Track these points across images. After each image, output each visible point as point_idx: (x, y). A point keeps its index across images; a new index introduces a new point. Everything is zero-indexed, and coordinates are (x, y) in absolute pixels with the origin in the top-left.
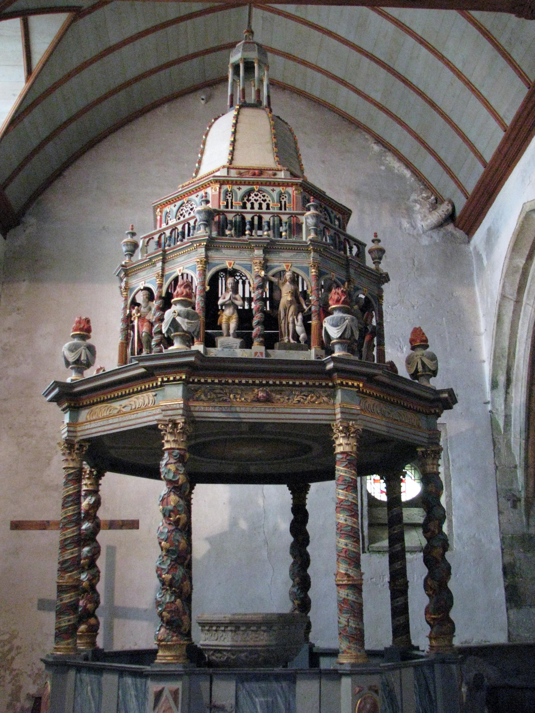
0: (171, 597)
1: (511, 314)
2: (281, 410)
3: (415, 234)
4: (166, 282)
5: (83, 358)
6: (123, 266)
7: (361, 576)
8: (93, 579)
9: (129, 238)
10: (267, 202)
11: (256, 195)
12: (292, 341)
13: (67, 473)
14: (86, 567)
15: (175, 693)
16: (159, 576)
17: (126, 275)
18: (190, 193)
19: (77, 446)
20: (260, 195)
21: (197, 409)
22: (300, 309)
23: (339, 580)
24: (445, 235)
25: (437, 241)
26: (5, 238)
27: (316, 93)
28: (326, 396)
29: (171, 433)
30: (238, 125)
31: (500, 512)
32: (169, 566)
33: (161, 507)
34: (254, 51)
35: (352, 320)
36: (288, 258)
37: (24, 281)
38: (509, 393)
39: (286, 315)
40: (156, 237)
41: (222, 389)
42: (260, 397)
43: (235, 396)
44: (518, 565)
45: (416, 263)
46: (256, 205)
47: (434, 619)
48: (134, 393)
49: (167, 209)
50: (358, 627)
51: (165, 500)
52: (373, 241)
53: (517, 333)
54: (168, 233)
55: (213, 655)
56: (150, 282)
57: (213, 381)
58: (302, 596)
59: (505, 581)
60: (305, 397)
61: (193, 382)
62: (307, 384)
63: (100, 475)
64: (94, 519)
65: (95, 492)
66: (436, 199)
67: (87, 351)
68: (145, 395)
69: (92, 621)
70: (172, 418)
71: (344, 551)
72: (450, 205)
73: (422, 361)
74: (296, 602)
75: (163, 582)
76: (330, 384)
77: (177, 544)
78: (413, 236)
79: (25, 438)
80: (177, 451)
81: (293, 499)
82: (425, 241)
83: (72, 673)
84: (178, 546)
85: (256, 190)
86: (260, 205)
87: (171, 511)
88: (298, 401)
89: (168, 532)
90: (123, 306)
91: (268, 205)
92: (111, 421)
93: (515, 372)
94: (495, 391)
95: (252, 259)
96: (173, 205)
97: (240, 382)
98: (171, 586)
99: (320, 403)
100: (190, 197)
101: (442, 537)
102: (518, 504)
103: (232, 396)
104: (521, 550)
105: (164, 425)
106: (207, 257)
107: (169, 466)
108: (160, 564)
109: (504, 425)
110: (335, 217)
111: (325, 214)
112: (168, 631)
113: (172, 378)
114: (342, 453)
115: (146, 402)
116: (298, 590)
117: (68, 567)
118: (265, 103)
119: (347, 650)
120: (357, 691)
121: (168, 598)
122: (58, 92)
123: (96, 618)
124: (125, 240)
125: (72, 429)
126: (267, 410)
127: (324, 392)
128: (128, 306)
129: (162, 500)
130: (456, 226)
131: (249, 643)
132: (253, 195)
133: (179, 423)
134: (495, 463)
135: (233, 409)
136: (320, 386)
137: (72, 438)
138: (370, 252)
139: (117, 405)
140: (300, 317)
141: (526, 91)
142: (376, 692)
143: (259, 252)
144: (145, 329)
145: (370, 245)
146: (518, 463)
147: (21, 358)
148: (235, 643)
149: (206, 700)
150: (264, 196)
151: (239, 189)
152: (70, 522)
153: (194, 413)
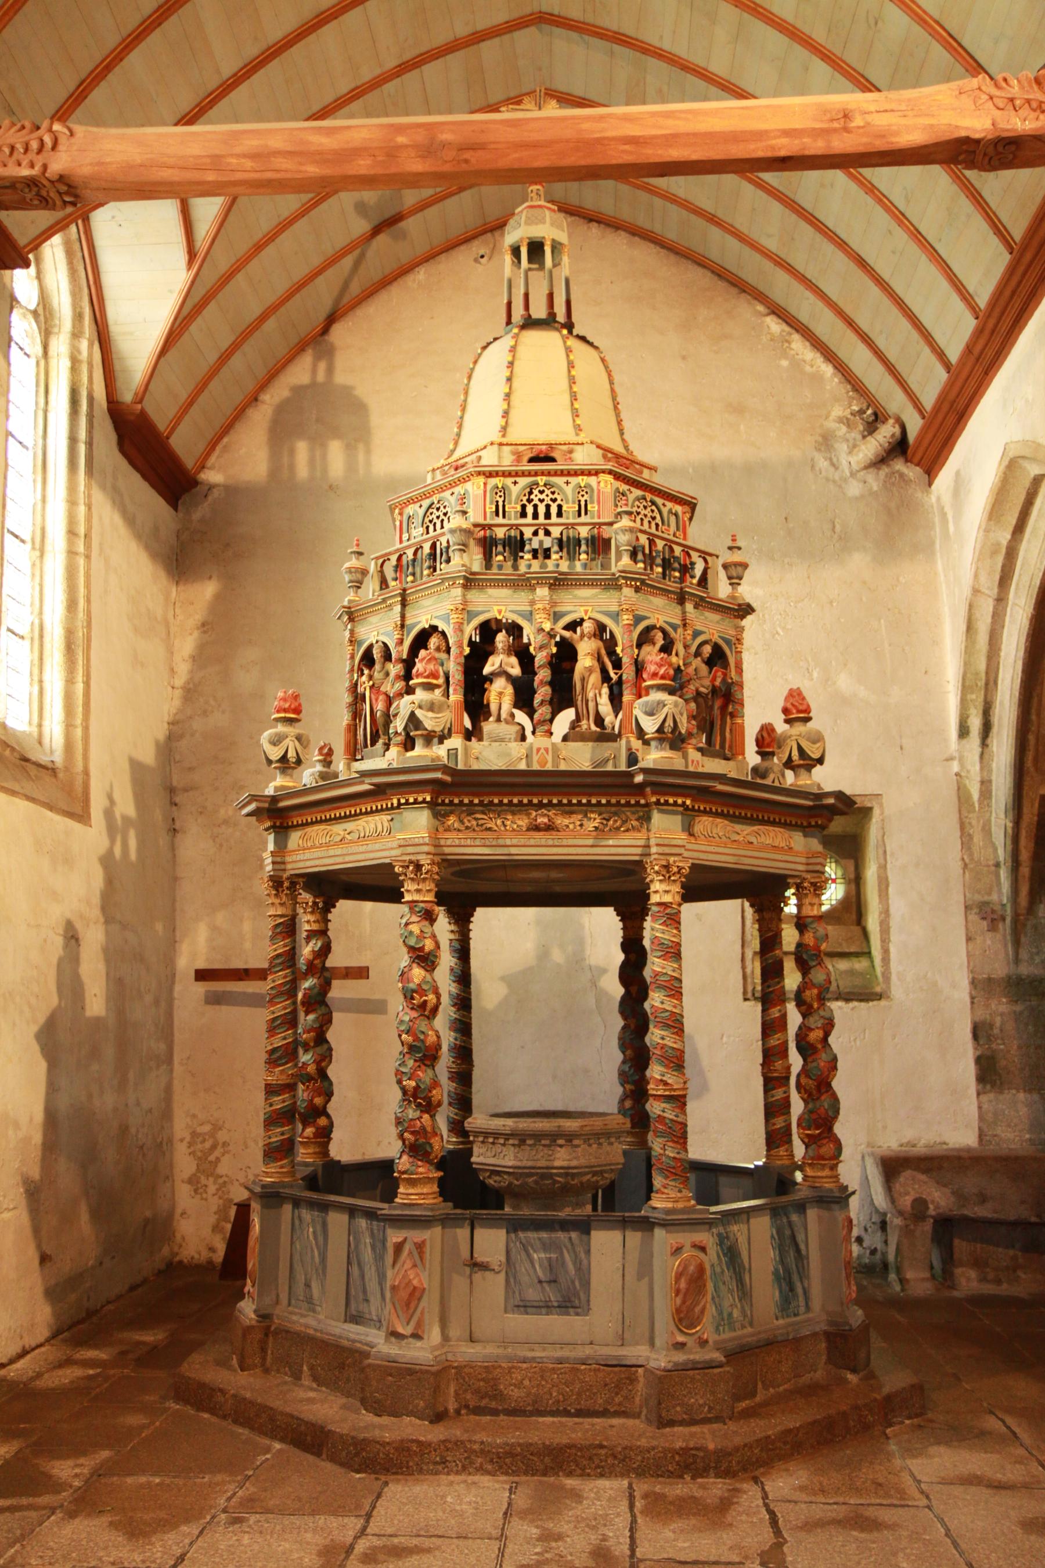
1: (989, 620)
2: (571, 842)
3: (837, 478)
4: (408, 635)
5: (291, 754)
6: (344, 607)
7: (685, 1083)
8: (323, 1060)
9: (354, 562)
10: (559, 502)
11: (541, 492)
12: (594, 728)
13: (273, 923)
14: (312, 1044)
16: (399, 1082)
17: (351, 619)
18: (442, 489)
19: (286, 884)
20: (547, 492)
21: (449, 842)
22: (606, 678)
25: (875, 488)
26: (176, 508)
27: (671, 234)
28: (637, 820)
29: (412, 879)
30: (516, 363)
31: (969, 939)
33: (400, 985)
34: (544, 223)
35: (676, 705)
36: (588, 598)
37: (210, 578)
38: (987, 746)
40: (394, 558)
41: (484, 813)
44: (998, 1024)
45: (838, 528)
46: (542, 509)
47: (808, 1135)
48: (361, 814)
49: (410, 510)
50: (677, 1156)
52: (730, 548)
53: (1000, 649)
54: (410, 553)
55: (489, 1177)
56: (384, 634)
57: (471, 802)
58: (637, 1077)
59: (976, 1049)
60: (605, 822)
61: (443, 803)
62: (608, 802)
63: (329, 905)
64: (322, 973)
65: (323, 933)
66: (875, 414)
67: (297, 742)
68: (377, 818)
69: (322, 1121)
70: (413, 858)
71: (659, 1047)
72: (897, 426)
73: (798, 744)
74: (628, 1087)
76: (643, 802)
78: (834, 481)
79: (224, 827)
80: (422, 905)
81: (624, 929)
82: (854, 489)
83: (287, 1208)
85: (542, 483)
86: (548, 507)
87: (413, 991)
90: (348, 669)
91: (560, 507)
92: (332, 853)
93: (997, 711)
94: (964, 741)
95: (532, 603)
96: (418, 504)
97: (511, 802)
98: (415, 1096)
99: (627, 830)
100: (442, 495)
101: (822, 1013)
102: (1001, 926)
103: (499, 822)
104: (1004, 1000)
105: (402, 867)
106: (465, 602)
107: (412, 927)
109: (979, 799)
110: (670, 511)
111: (653, 511)
112: (411, 1160)
113: (411, 800)
114: (659, 904)
115: (380, 829)
116: (630, 1068)
117: (280, 1058)
118: (561, 317)
119: (663, 1190)
122: (240, 277)
123: (328, 1116)
124: (347, 565)
125: (278, 859)
126: (550, 842)
127: (633, 813)
128: (356, 668)
129: (402, 975)
131: (539, 1164)
132: (536, 492)
133: (423, 865)
134: (963, 859)
135: (501, 842)
136: (628, 804)
137: (280, 873)
138: (725, 566)
139: (339, 829)
140: (605, 690)
141: (1006, 258)
142: (703, 1249)
144: (380, 706)
146: (1001, 859)
147: (212, 702)
148: (519, 1164)
149: (465, 1253)
150: (553, 493)
151: (515, 483)
152: (280, 994)
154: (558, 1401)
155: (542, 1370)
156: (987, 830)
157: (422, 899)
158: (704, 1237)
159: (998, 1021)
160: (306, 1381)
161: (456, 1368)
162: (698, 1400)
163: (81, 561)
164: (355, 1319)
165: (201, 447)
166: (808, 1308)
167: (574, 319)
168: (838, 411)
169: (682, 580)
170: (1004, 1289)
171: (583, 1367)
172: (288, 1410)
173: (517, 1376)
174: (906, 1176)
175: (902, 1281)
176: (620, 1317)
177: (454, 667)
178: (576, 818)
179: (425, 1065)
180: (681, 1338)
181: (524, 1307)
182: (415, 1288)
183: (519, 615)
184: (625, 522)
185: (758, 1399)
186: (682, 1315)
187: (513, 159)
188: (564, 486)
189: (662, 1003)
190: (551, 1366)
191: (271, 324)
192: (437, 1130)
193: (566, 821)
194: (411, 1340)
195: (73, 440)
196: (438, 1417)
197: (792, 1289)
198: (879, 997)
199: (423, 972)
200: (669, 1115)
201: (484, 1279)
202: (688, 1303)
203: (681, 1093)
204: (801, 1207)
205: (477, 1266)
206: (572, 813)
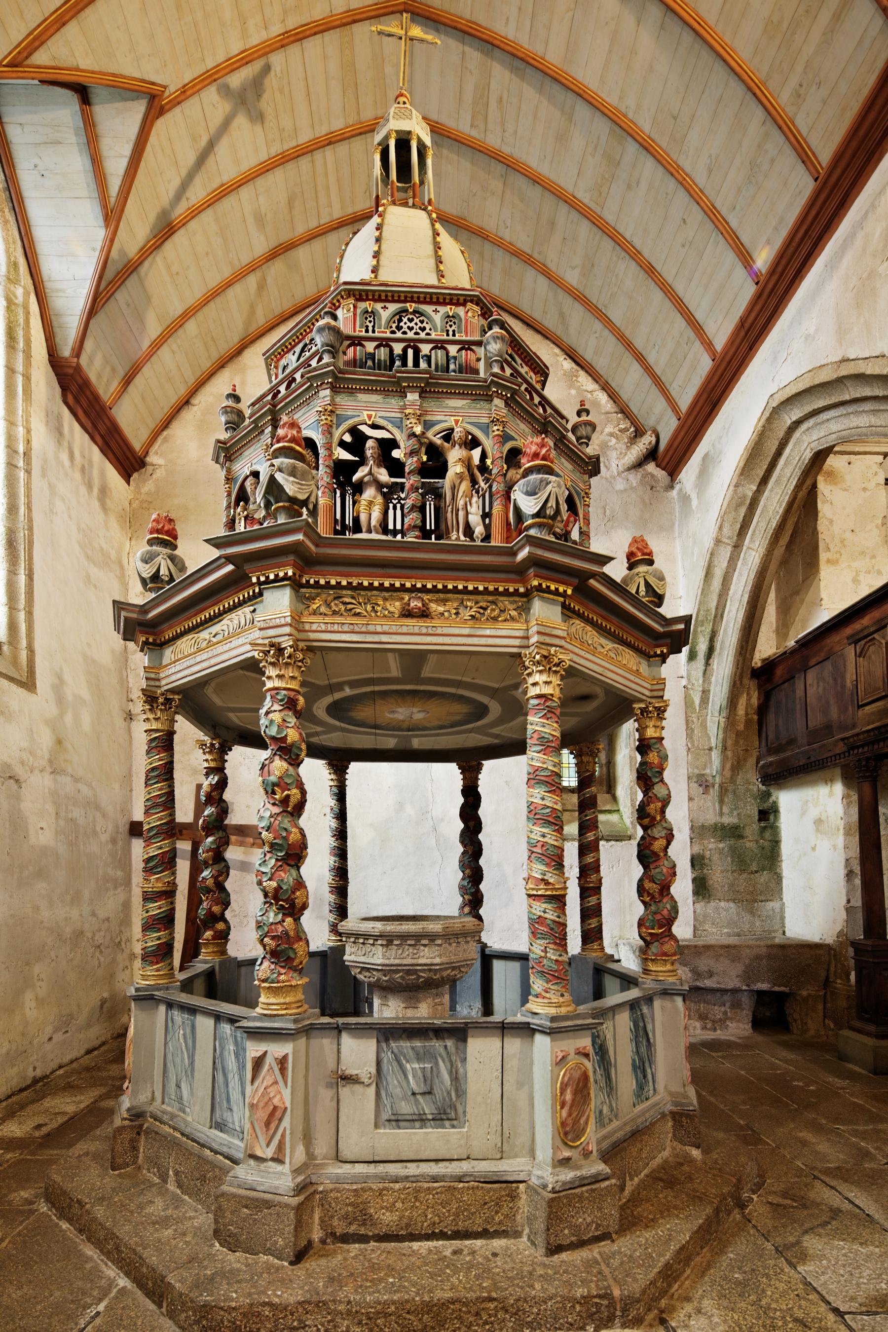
0: (276, 915)
7: (565, 883)
10: (427, 331)
11: (411, 320)
16: (260, 883)
23: (533, 889)
32: (272, 868)
33: (261, 779)
41: (353, 598)
42: (413, 608)
43: (373, 607)
50: (560, 959)
51: (266, 768)
71: (539, 845)
77: (284, 834)
80: (284, 692)
84: (285, 839)
88: (471, 616)
89: (271, 816)
98: (276, 898)
103: (369, 608)
108: (260, 865)
112: (273, 966)
119: (544, 994)
120: (560, 1058)
121: (272, 917)
126: (424, 631)
127: (511, 602)
129: (262, 768)
132: (405, 320)
135: (371, 628)
150: (422, 322)
153: (309, 634)
154: (434, 1223)
155: (417, 1191)
157: (284, 685)
161: (321, 1192)
171: (461, 1185)
173: (389, 1198)
176: (499, 1128)
178: (451, 606)
179: (289, 865)
180: (567, 1154)
182: (275, 1108)
183: (389, 421)
186: (568, 1129)
188: (433, 314)
189: (543, 799)
190: (426, 1185)
192: (301, 934)
193: (441, 609)
194: (270, 1163)
199: (285, 765)
201: (353, 1093)
202: (574, 1115)
203: (562, 893)
206: (446, 600)
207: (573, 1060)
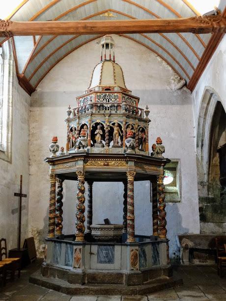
5: (55, 149)
9: (68, 110)
15: (80, 250)
18: (87, 95)
22: (120, 135)
24: (183, 91)
31: (199, 190)
35: (133, 141)
39: (115, 137)
46: (107, 100)
49: (81, 99)
54: (80, 108)
63: (63, 181)
65: (61, 186)
66: (180, 78)
69: (61, 226)
75: (77, 218)
82: (175, 94)
118: (112, 59)
130: (187, 88)
139: (65, 165)
140: (119, 137)
142: (137, 250)
143: (107, 117)
144: (74, 140)
145: (145, 110)
156: (202, 167)
158: (137, 248)
159: (204, 207)
160: (57, 278)
162: (135, 280)
163: (11, 108)
164: (67, 265)
165: (36, 82)
166: (159, 264)
167: (115, 60)
168: (172, 78)
169: (136, 114)
170: (204, 264)
172: (53, 283)
174: (184, 239)
175: (183, 262)
177: (89, 132)
180: (132, 268)
181: (101, 262)
184: (124, 103)
185: (148, 282)
187: (102, 30)
191: (51, 58)
195: (9, 82)
196: (83, 284)
197: (156, 260)
198: (180, 202)
200: (131, 223)
204: (159, 243)
205: (91, 253)
207: (134, 251)
